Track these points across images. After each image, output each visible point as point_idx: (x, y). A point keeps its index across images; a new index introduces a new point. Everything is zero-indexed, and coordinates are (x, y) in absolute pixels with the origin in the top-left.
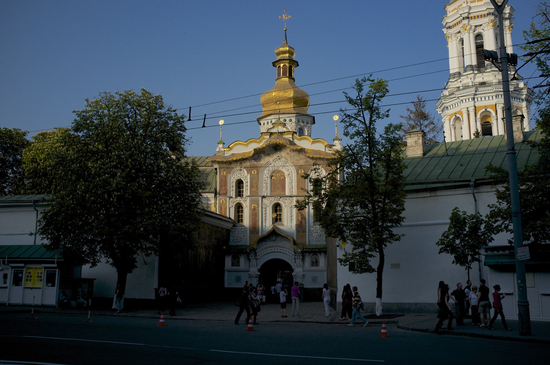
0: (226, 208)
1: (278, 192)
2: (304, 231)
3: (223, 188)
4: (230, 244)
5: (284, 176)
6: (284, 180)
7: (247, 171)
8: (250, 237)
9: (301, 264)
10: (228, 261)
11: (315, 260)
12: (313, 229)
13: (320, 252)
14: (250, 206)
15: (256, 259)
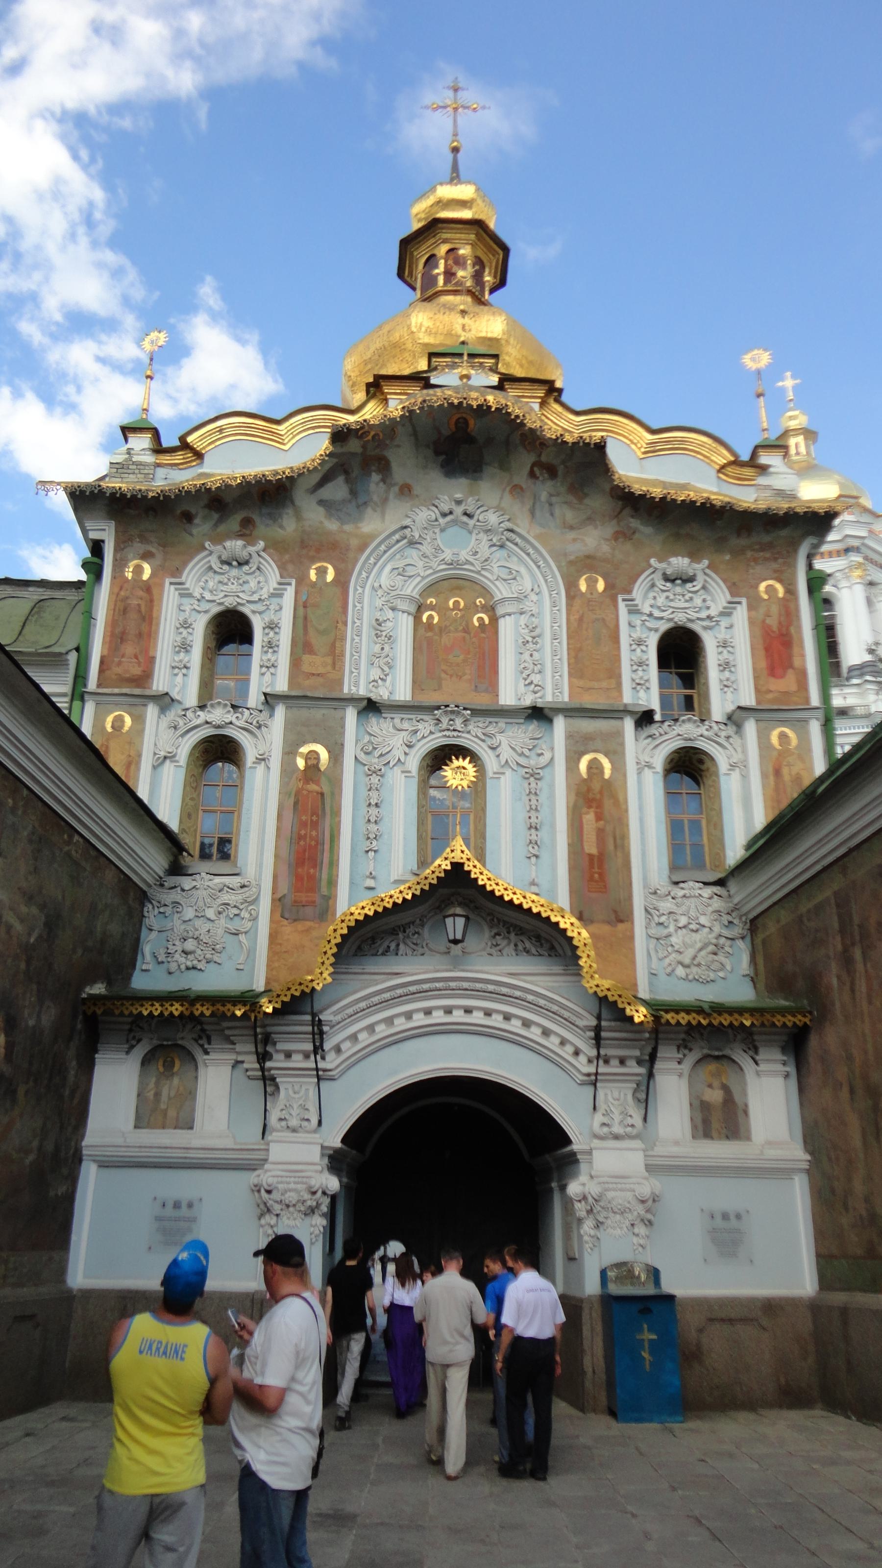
0: (133, 762)
1: (455, 691)
2: (621, 916)
3: (129, 649)
4: (140, 982)
5: (490, 609)
6: (492, 629)
7: (282, 568)
8: (273, 937)
9: (637, 1120)
10: (115, 1086)
11: (715, 1096)
12: (666, 905)
13: (750, 1041)
14: (290, 752)
15: (320, 1076)
